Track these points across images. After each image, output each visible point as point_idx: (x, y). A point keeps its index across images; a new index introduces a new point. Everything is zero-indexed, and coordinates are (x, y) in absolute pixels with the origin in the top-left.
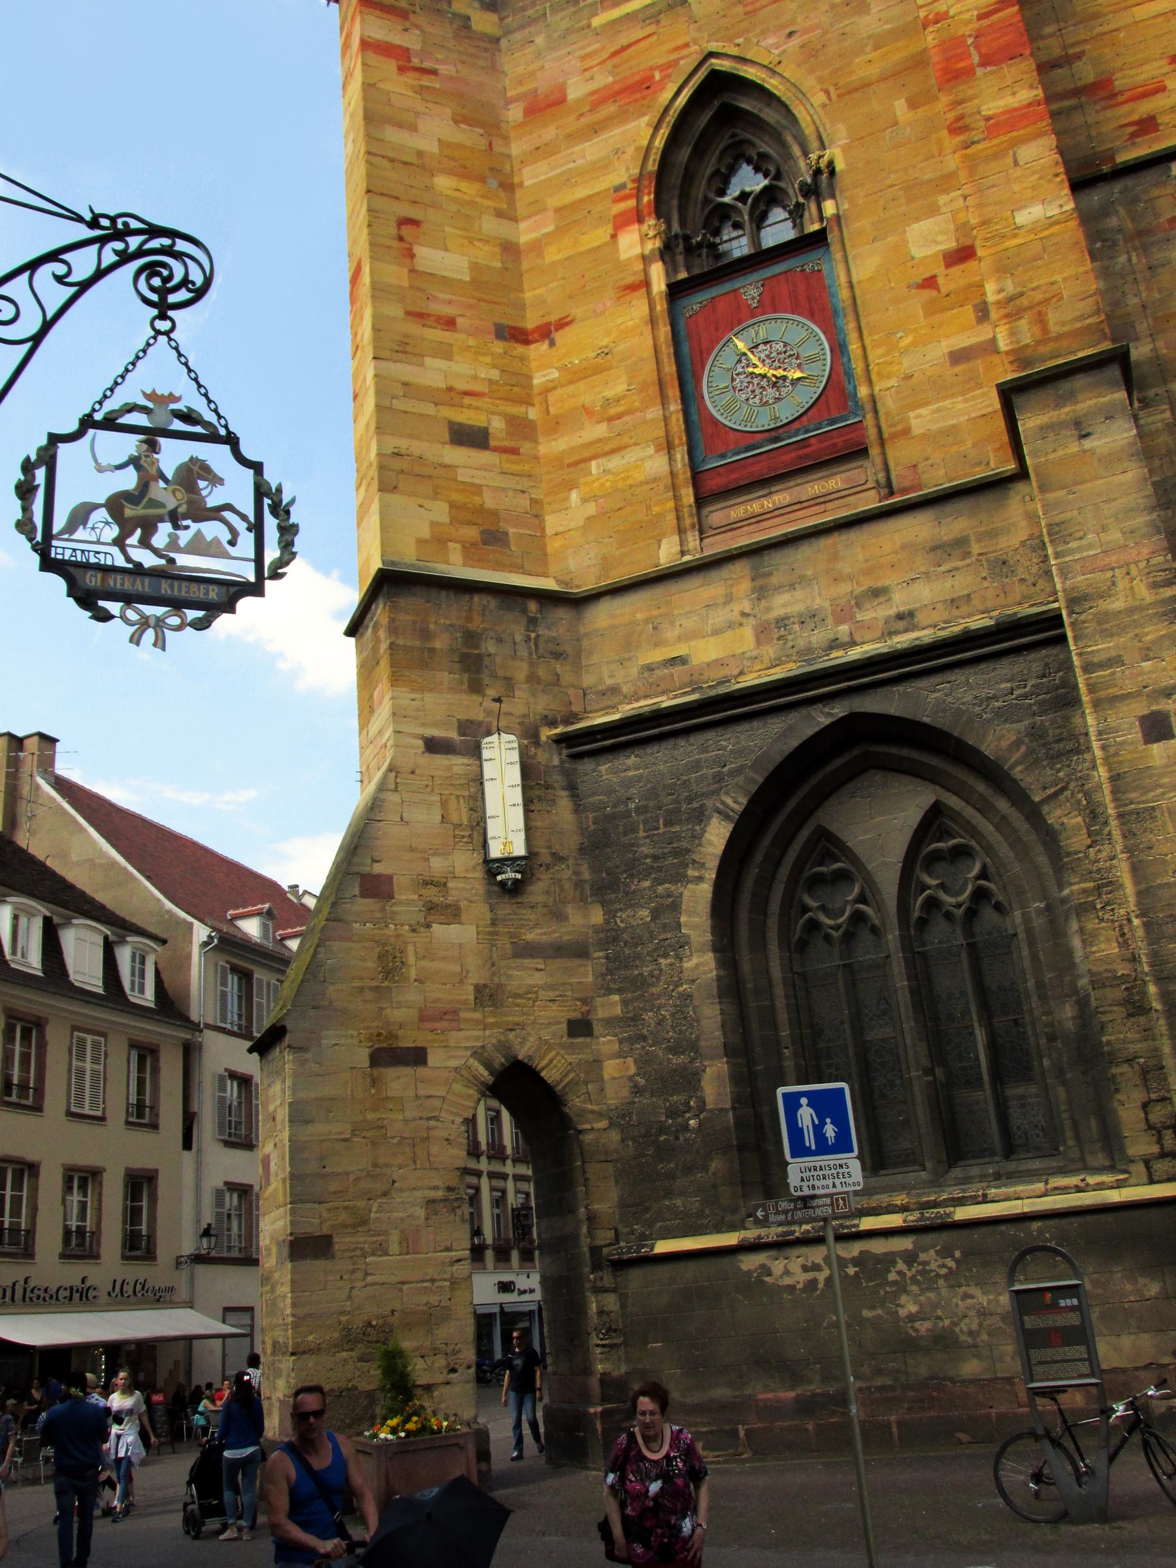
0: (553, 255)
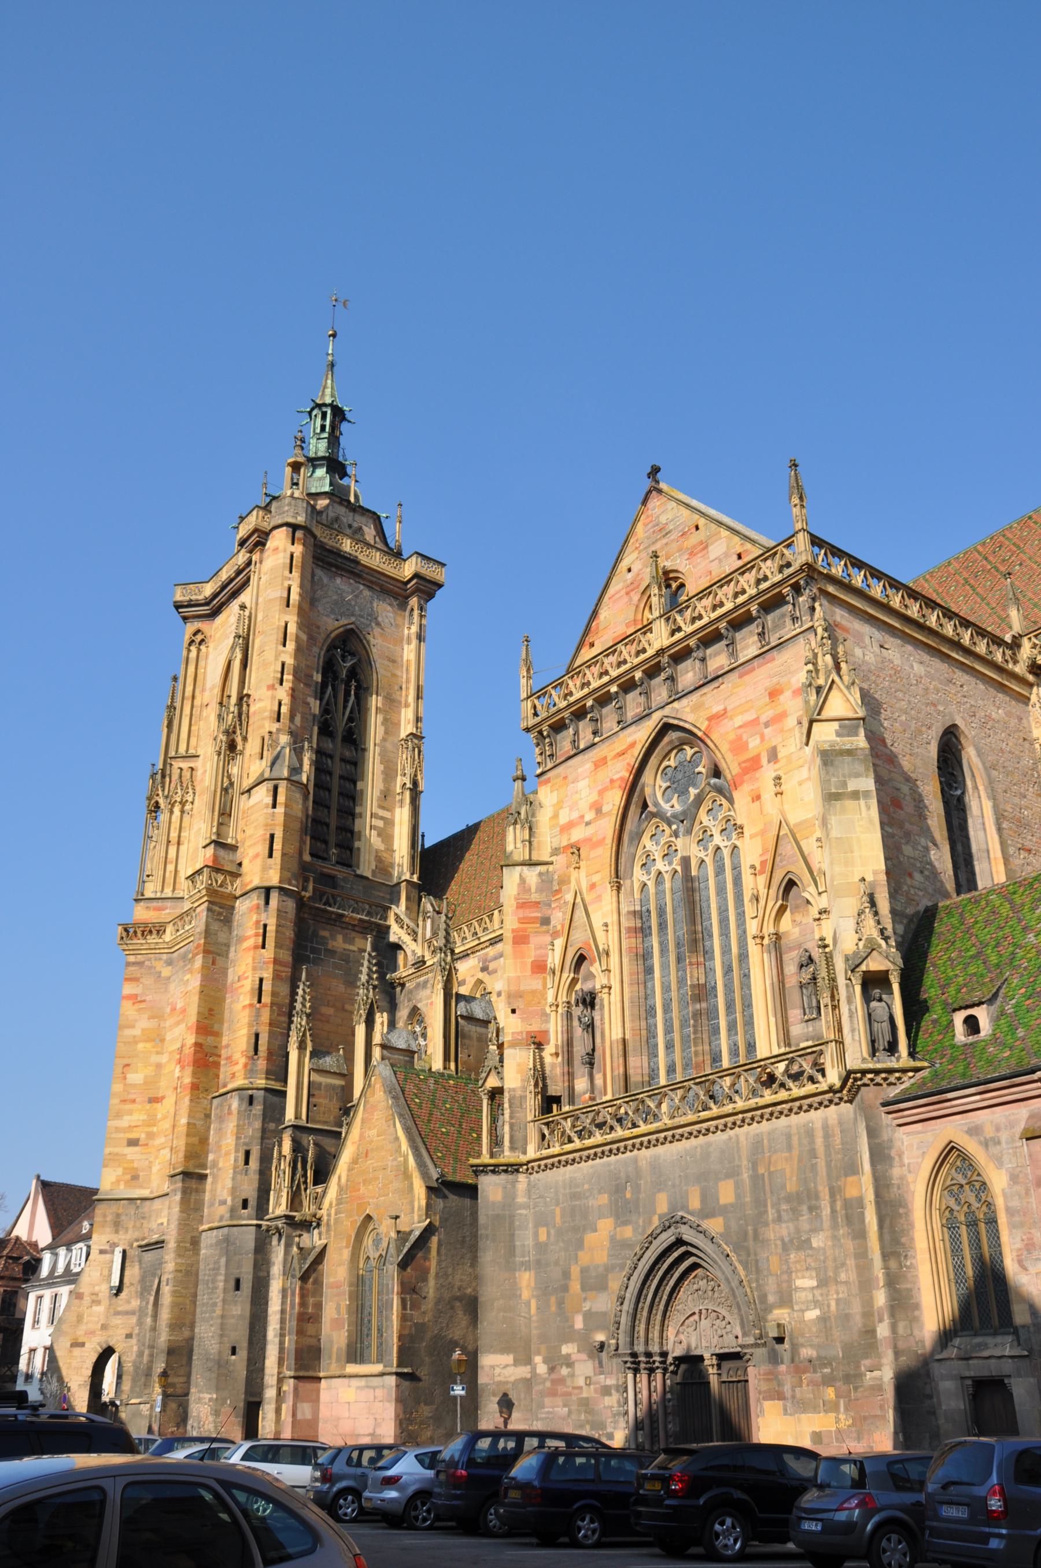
0: (167, 1071)
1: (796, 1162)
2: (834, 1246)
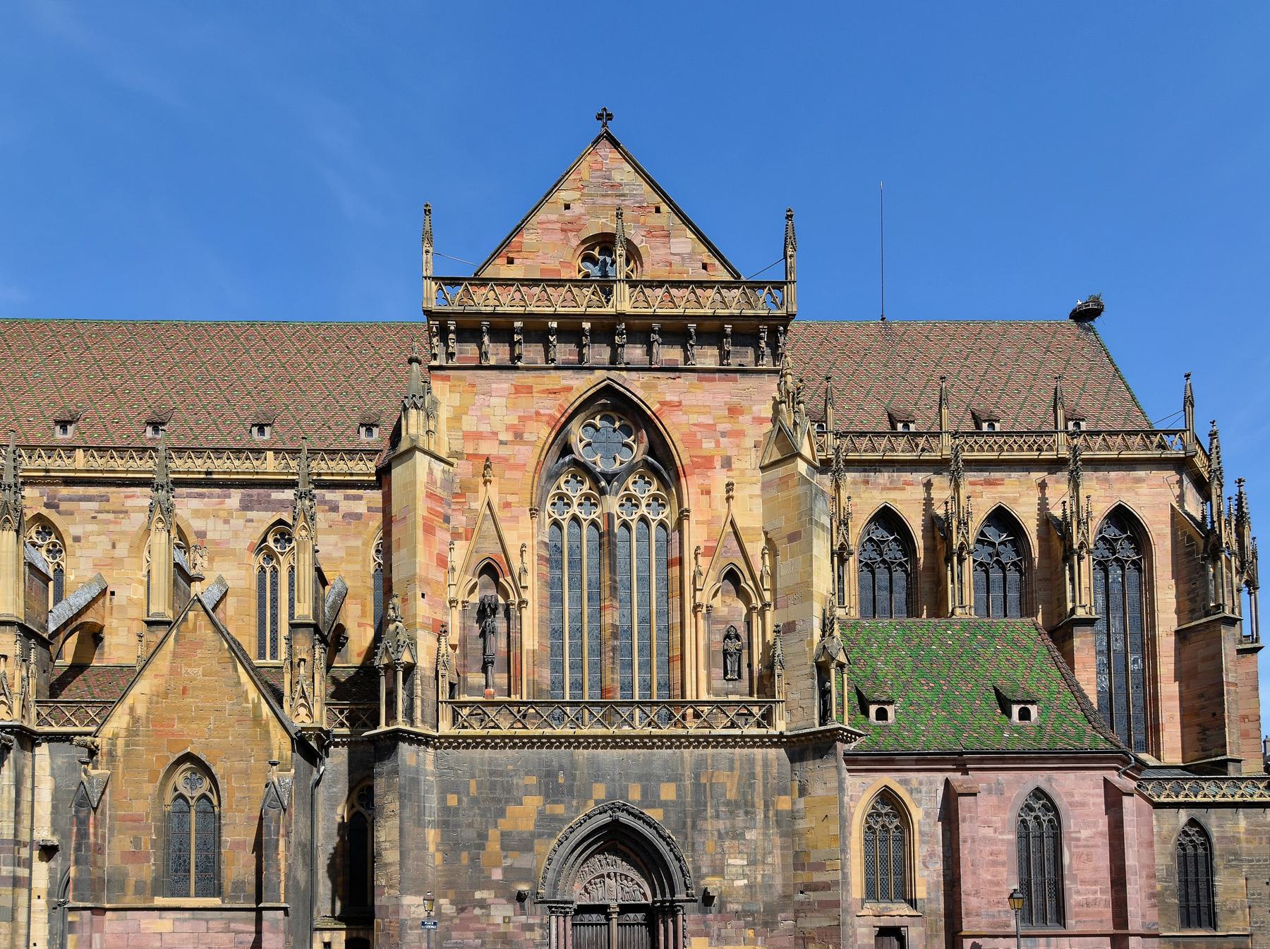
1: (736, 779)
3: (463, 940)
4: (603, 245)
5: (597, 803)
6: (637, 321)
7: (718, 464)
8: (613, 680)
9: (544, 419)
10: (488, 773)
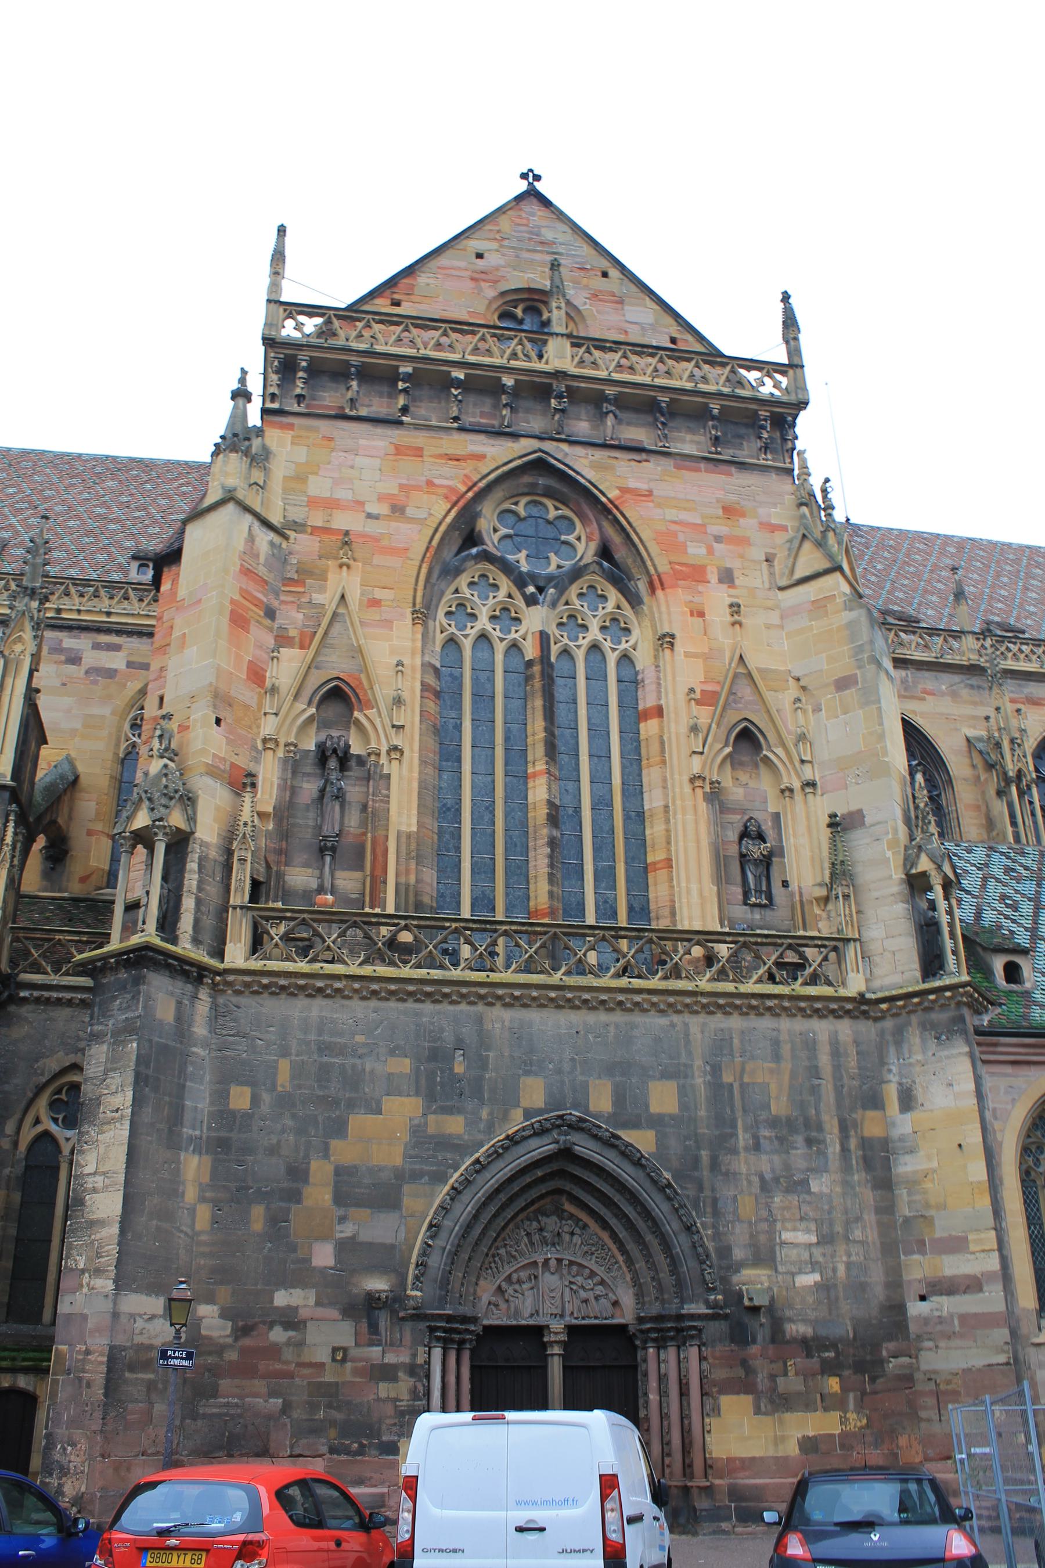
1: (786, 1077)
2: (844, 1194)
3: (242, 1397)
4: (529, 303)
5: (528, 1114)
6: (583, 385)
7: (713, 577)
8: (551, 894)
9: (441, 491)
10: (314, 1047)
